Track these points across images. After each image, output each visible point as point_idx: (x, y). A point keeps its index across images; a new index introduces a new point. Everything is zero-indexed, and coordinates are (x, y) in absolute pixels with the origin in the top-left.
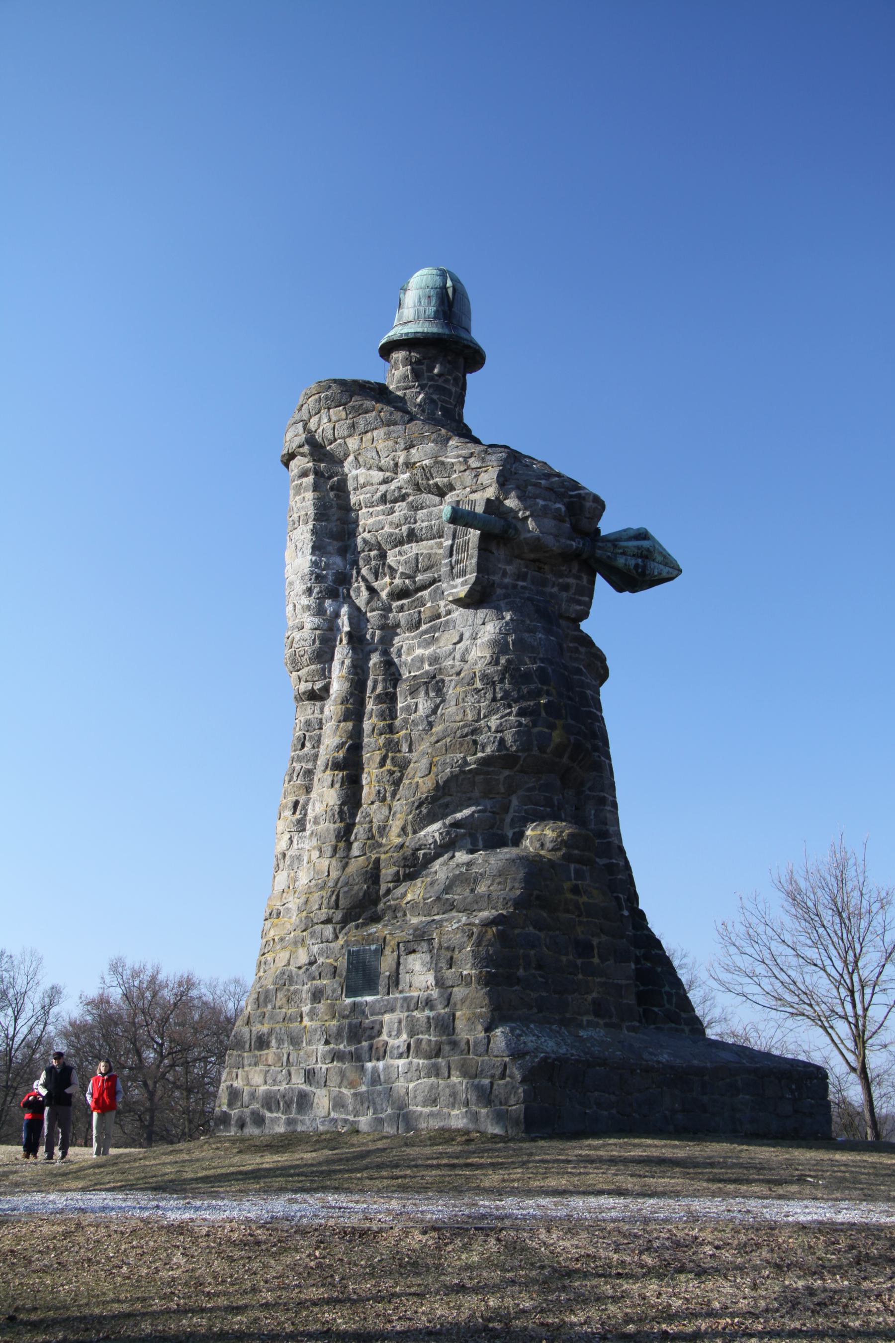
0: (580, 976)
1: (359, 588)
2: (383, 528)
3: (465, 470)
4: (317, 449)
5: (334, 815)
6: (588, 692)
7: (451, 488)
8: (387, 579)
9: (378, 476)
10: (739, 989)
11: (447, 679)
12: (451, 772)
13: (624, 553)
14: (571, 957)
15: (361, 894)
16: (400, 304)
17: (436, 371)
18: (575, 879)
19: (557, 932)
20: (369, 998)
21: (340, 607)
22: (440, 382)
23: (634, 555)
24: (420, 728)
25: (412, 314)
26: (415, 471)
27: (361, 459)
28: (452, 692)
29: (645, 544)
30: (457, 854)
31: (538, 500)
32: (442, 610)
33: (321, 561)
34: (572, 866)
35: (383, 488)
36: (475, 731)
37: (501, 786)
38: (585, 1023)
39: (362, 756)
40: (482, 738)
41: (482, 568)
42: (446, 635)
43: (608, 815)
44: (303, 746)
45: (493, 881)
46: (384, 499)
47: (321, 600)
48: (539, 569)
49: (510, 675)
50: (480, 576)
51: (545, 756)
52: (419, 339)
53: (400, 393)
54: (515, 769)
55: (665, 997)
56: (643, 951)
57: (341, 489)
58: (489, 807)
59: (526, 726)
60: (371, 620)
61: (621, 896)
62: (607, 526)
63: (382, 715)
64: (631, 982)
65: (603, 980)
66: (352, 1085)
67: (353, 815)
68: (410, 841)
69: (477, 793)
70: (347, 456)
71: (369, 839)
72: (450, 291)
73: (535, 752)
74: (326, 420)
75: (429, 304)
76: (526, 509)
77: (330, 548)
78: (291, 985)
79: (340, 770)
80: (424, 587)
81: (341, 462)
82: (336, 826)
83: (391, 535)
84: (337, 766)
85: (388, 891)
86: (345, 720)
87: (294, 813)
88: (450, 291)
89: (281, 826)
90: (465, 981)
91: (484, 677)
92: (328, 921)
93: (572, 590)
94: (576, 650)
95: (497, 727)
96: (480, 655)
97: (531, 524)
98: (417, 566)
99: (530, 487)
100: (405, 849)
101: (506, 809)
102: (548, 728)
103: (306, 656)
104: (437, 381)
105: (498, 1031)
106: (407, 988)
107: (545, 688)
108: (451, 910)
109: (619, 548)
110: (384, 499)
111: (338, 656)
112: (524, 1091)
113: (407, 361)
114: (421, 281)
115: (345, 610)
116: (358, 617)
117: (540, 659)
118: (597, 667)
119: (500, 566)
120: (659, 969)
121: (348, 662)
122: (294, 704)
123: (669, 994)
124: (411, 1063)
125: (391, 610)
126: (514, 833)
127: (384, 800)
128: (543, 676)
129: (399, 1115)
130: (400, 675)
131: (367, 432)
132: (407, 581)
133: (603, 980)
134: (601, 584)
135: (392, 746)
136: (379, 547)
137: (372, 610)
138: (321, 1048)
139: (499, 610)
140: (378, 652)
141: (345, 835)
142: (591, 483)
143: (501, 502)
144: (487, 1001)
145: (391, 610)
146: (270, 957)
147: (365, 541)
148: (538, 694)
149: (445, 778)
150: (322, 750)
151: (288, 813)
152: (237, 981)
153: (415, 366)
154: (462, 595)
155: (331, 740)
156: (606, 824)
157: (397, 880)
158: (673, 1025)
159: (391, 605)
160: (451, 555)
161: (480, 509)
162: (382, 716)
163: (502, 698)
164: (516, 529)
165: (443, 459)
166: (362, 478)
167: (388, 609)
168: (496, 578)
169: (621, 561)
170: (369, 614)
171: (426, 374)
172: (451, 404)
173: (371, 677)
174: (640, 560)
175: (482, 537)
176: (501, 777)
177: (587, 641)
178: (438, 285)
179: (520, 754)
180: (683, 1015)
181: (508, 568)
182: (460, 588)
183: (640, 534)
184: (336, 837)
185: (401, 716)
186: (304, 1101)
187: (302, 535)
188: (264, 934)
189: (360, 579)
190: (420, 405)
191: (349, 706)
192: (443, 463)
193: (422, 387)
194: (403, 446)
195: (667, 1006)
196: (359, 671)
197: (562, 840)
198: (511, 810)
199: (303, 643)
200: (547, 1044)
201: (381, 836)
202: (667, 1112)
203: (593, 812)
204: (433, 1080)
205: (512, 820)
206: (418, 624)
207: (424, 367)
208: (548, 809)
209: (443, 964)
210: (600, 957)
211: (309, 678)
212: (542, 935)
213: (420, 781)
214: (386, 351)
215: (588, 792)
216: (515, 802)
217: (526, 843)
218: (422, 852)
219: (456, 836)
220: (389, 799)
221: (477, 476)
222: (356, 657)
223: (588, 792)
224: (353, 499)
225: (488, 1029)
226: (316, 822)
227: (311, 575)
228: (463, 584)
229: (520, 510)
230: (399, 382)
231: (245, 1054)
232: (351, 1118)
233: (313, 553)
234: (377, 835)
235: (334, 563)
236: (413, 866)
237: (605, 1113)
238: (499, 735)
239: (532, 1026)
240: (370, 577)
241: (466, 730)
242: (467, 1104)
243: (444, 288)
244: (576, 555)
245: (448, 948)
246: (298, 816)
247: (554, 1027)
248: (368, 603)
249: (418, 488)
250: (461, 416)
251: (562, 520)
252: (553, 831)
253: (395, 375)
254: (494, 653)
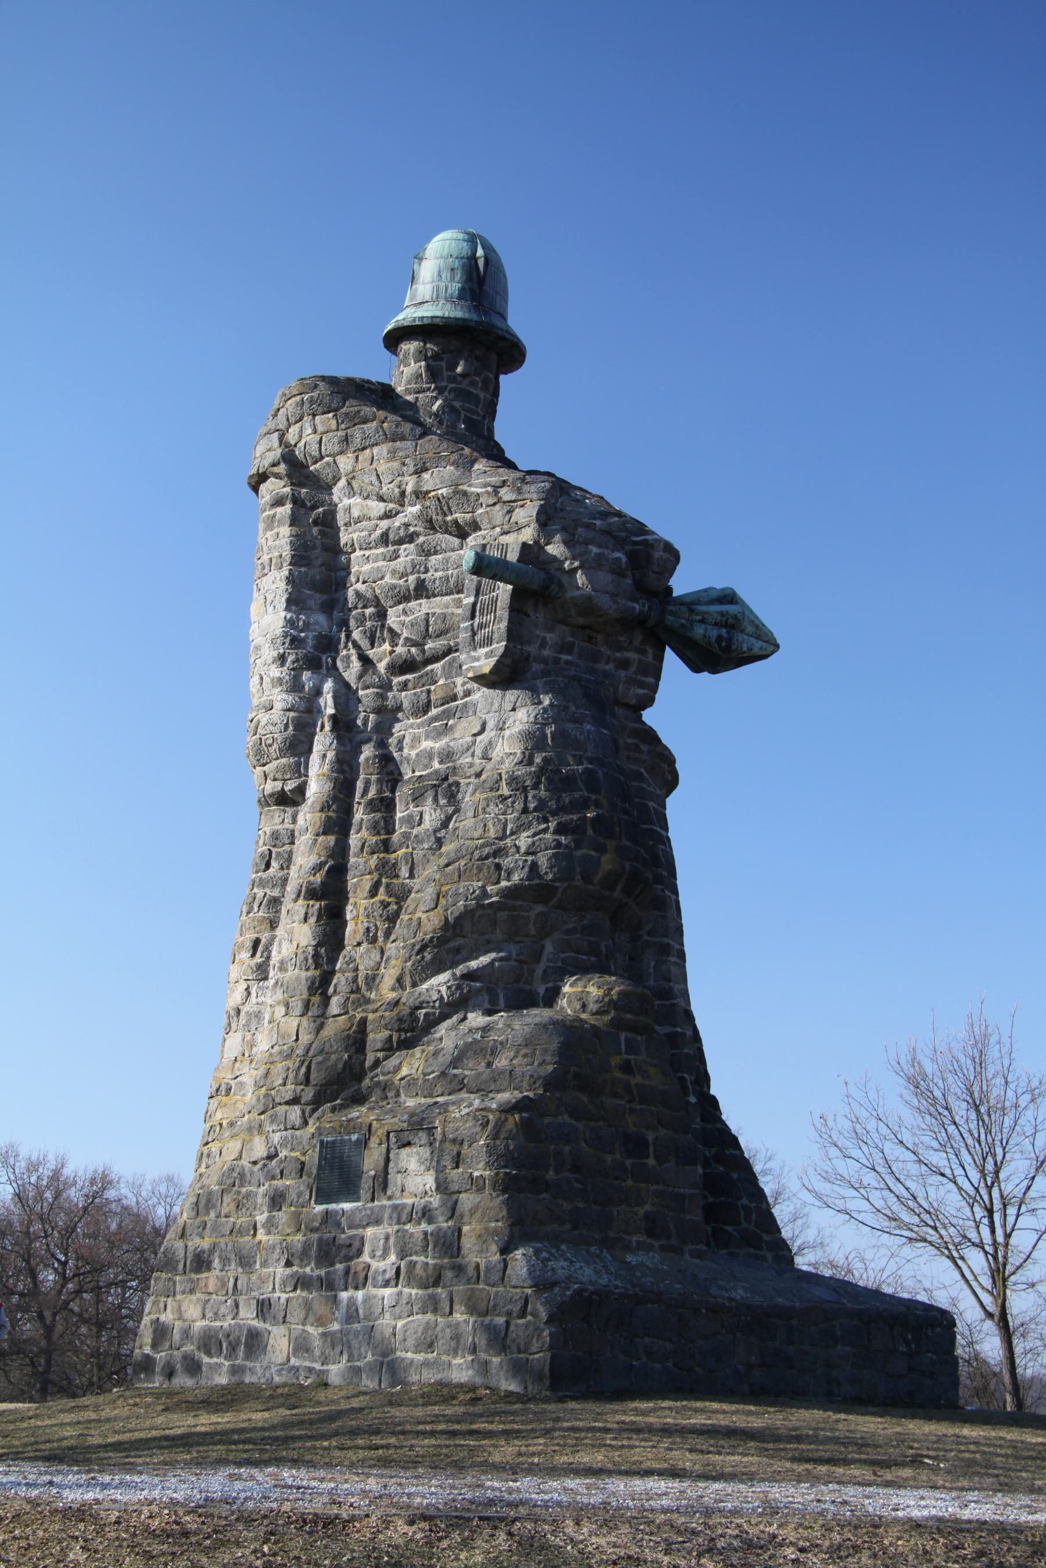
0: (630, 1182)
1: (348, 657)
2: (382, 578)
3: (494, 504)
4: (295, 467)
5: (306, 960)
6: (651, 804)
7: (476, 527)
8: (387, 646)
9: (377, 508)
10: (840, 1204)
11: (463, 781)
12: (465, 906)
13: (703, 621)
14: (618, 1156)
15: (340, 1066)
16: (413, 278)
17: (459, 370)
18: (627, 1053)
19: (601, 1123)
20: (347, 1206)
21: (322, 682)
22: (465, 385)
23: (716, 624)
24: (426, 846)
25: (428, 290)
26: (428, 503)
27: (354, 483)
28: (468, 799)
29: (732, 609)
30: (470, 1015)
31: (590, 547)
32: (460, 690)
33: (299, 620)
34: (623, 1036)
35: (384, 524)
36: (498, 853)
37: (531, 926)
38: (634, 1244)
39: (347, 881)
40: (507, 862)
41: (512, 634)
42: (464, 723)
43: (672, 968)
44: (268, 866)
45: (517, 1052)
46: (385, 539)
47: (296, 672)
48: (590, 639)
49: (548, 779)
50: (511, 645)
51: (591, 887)
52: (437, 326)
53: (410, 398)
54: (551, 904)
55: (742, 1213)
56: (714, 1150)
57: (328, 523)
58: (514, 954)
59: (566, 847)
60: (364, 700)
61: (686, 1076)
62: (683, 583)
63: (375, 828)
64: (697, 1191)
65: (660, 1187)
66: (320, 1322)
67: (333, 960)
68: (408, 997)
69: (498, 935)
70: (336, 479)
71: (352, 992)
72: (481, 263)
73: (578, 881)
74: (310, 431)
75: (452, 279)
76: (574, 558)
77: (311, 603)
78: (242, 1185)
79: (317, 900)
80: (435, 659)
81: (329, 488)
82: (310, 973)
83: (393, 587)
84: (312, 894)
85: (377, 1063)
86: (325, 833)
87: (253, 955)
88: (481, 263)
89: (235, 971)
90: (476, 1185)
91: (513, 780)
92: (295, 1101)
93: (633, 668)
94: (637, 748)
95: (529, 848)
96: (507, 751)
97: (580, 578)
98: (427, 630)
99: (580, 529)
100: (401, 1007)
101: (537, 957)
102: (596, 850)
103: (275, 746)
104: (460, 383)
105: (519, 1253)
106: (398, 1194)
107: (593, 797)
108: (460, 1090)
109: (697, 614)
110: (385, 539)
111: (318, 747)
112: (551, 1335)
113: (421, 355)
114: (441, 248)
115: (328, 686)
116: (346, 695)
117: (587, 758)
118: (664, 772)
119: (538, 633)
120: (735, 1176)
121: (331, 755)
122: (257, 809)
123: (747, 1210)
124: (400, 1294)
125: (390, 689)
126: (547, 990)
127: (373, 941)
128: (591, 781)
129: (382, 1364)
130: (400, 774)
131: (364, 449)
132: (413, 650)
133: (660, 1187)
134: (672, 662)
135: (388, 869)
136: (377, 603)
137: (367, 687)
138: (281, 1272)
139: (535, 693)
140: (372, 744)
141: (320, 987)
142: (662, 525)
143: (542, 548)
144: (504, 1213)
145: (390, 689)
146: (214, 1147)
147: (358, 595)
148: (584, 805)
149: (457, 914)
150: (293, 871)
151: (245, 955)
152: (170, 1179)
153: (431, 362)
154: (486, 670)
155: (306, 859)
156: (670, 981)
157: (389, 1048)
158: (752, 1250)
159: (390, 682)
160: (473, 617)
161: (513, 556)
162: (375, 828)
163: (535, 810)
164: (561, 585)
165: (465, 488)
166: (357, 510)
167: (386, 686)
168: (532, 649)
169: (699, 631)
170: (361, 693)
171: (445, 374)
172: (478, 414)
173: (362, 777)
174: (724, 631)
175: (515, 596)
176: (532, 915)
177: (650, 736)
178: (464, 253)
179: (557, 884)
180: (766, 1237)
181: (548, 636)
182: (484, 660)
183: (725, 597)
184: (309, 988)
185: (400, 829)
186: (255, 1343)
187: (275, 585)
188: (207, 1116)
189: (350, 645)
190: (436, 415)
191: (330, 814)
192: (465, 493)
193: (440, 390)
194: (412, 469)
195: (745, 1225)
196: (346, 768)
197: (611, 1001)
198: (544, 959)
199: (271, 728)
200: (586, 1272)
201: (370, 989)
202: (740, 1367)
203: (652, 964)
204: (429, 1316)
205: (545, 971)
206: (426, 708)
207: (444, 364)
208: (593, 959)
209: (447, 1162)
210: (656, 1157)
211: (279, 776)
212: (580, 1126)
213: (424, 916)
214: (394, 340)
215: (646, 937)
216: (549, 947)
217: (563, 1002)
218: (424, 1011)
219: (469, 991)
220: (381, 939)
221: (510, 512)
222: (342, 748)
223: (646, 937)
224: (344, 538)
225: (505, 1250)
226: (282, 967)
227: (285, 637)
228: (488, 656)
229: (566, 559)
230: (409, 382)
231: (178, 1278)
232: (317, 1366)
233: (287, 609)
234: (364, 988)
235: (316, 623)
236: (411, 1030)
237: (658, 1366)
238: (530, 858)
239: (563, 1247)
240: (364, 643)
241: (487, 850)
242: (474, 1350)
243: (473, 258)
244: (639, 622)
245: (454, 1141)
246: (258, 959)
247: (593, 1249)
248: (360, 677)
249: (431, 526)
250: (491, 431)
251: (623, 575)
252: (599, 987)
253: (404, 373)
254: (526, 749)
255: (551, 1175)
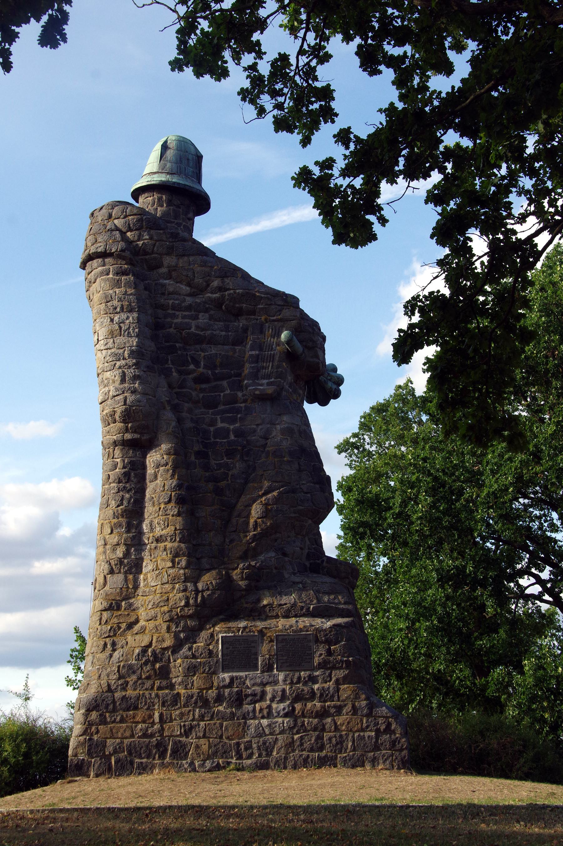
126: (311, 564)
131: (184, 255)
228: (268, 384)
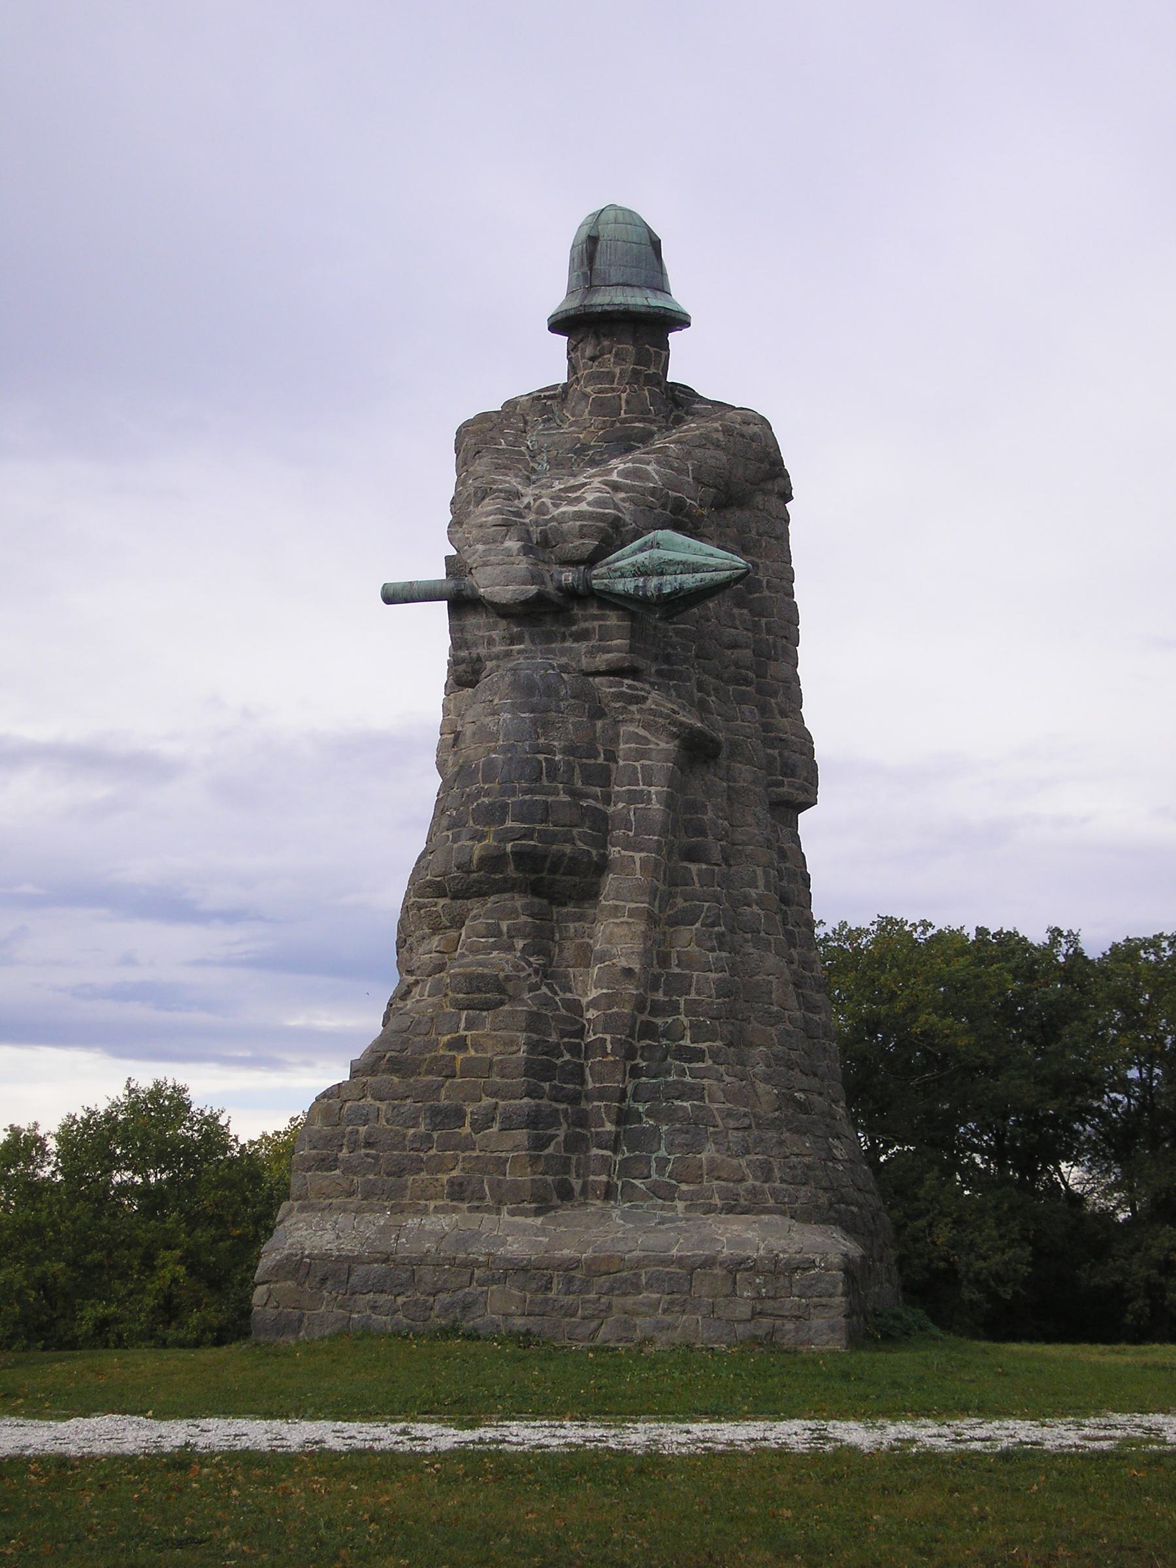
158: (660, 1201)
168: (482, 651)
195: (655, 1176)
212: (383, 1106)
255: (344, 1153)
